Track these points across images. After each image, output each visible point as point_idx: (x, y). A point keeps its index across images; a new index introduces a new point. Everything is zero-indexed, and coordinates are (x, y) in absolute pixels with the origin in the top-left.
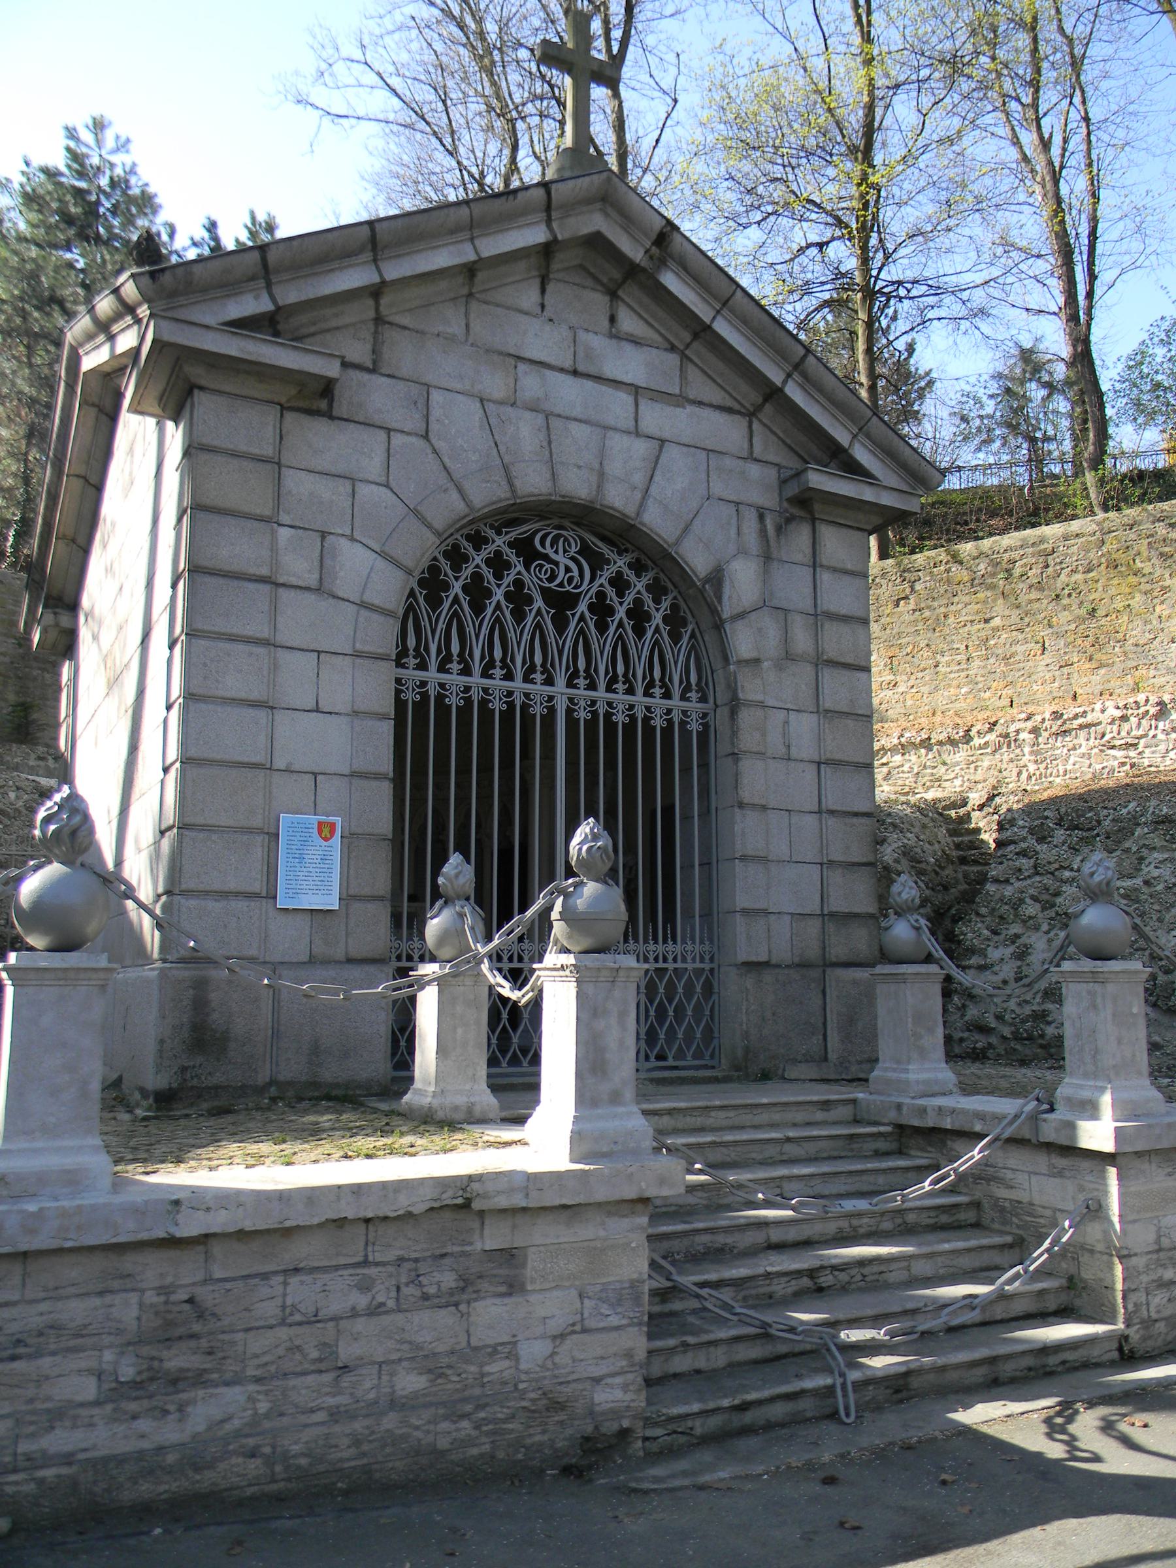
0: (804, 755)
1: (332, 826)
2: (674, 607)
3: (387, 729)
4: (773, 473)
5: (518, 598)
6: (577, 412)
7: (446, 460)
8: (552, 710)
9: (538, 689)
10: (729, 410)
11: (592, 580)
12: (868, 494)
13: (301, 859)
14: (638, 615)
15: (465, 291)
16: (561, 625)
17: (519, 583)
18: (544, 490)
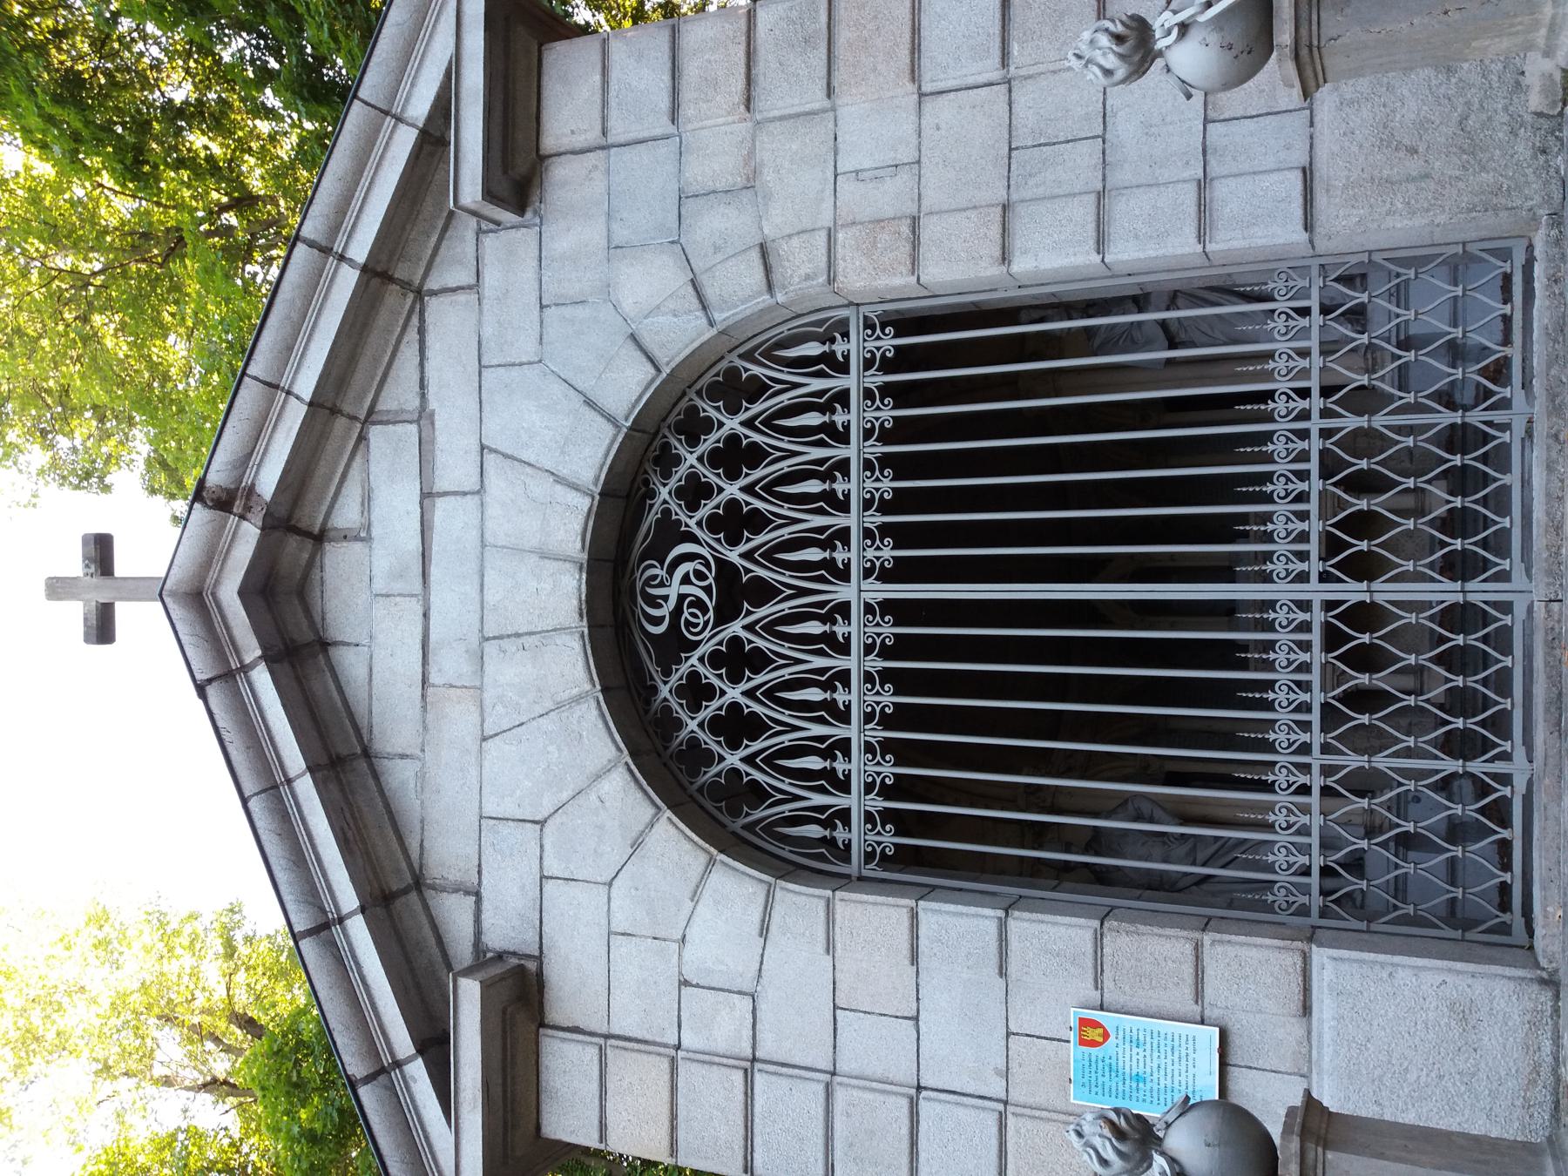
0: (909, 128)
1: (1085, 1023)
2: (713, 392)
4: (489, 241)
5: (736, 660)
6: (472, 590)
7: (565, 796)
8: (888, 607)
9: (854, 629)
10: (422, 331)
11: (693, 539)
13: (1138, 1078)
14: (734, 457)
15: (362, 765)
16: (763, 592)
17: (715, 660)
18: (577, 645)
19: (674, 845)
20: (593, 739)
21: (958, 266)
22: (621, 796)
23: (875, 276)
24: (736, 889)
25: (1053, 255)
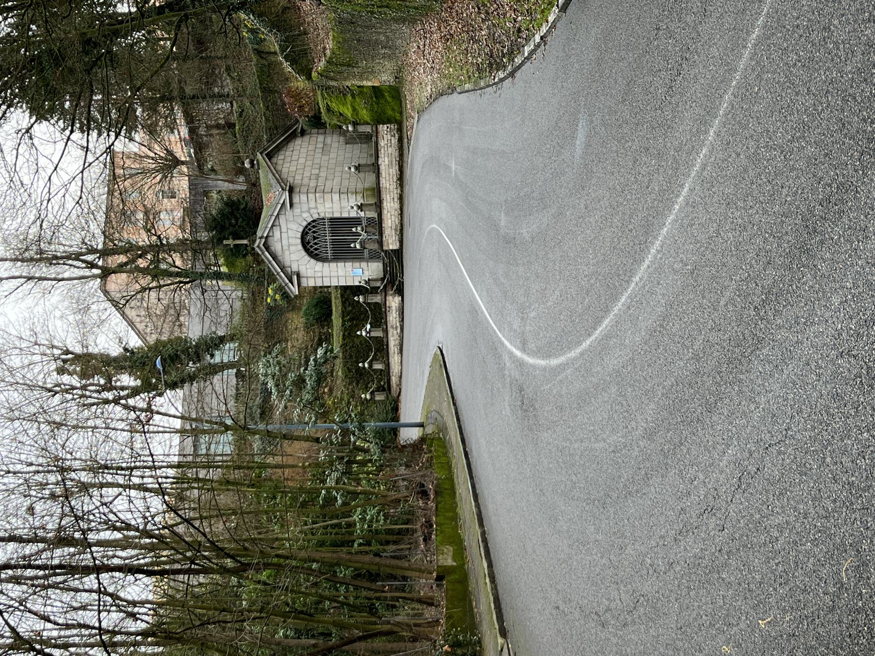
5: (316, 244)
14: (314, 227)
19: (313, 261)
20: (303, 253)
21: (337, 215)
22: (307, 258)
23: (329, 216)
24: (320, 264)
25: (345, 215)
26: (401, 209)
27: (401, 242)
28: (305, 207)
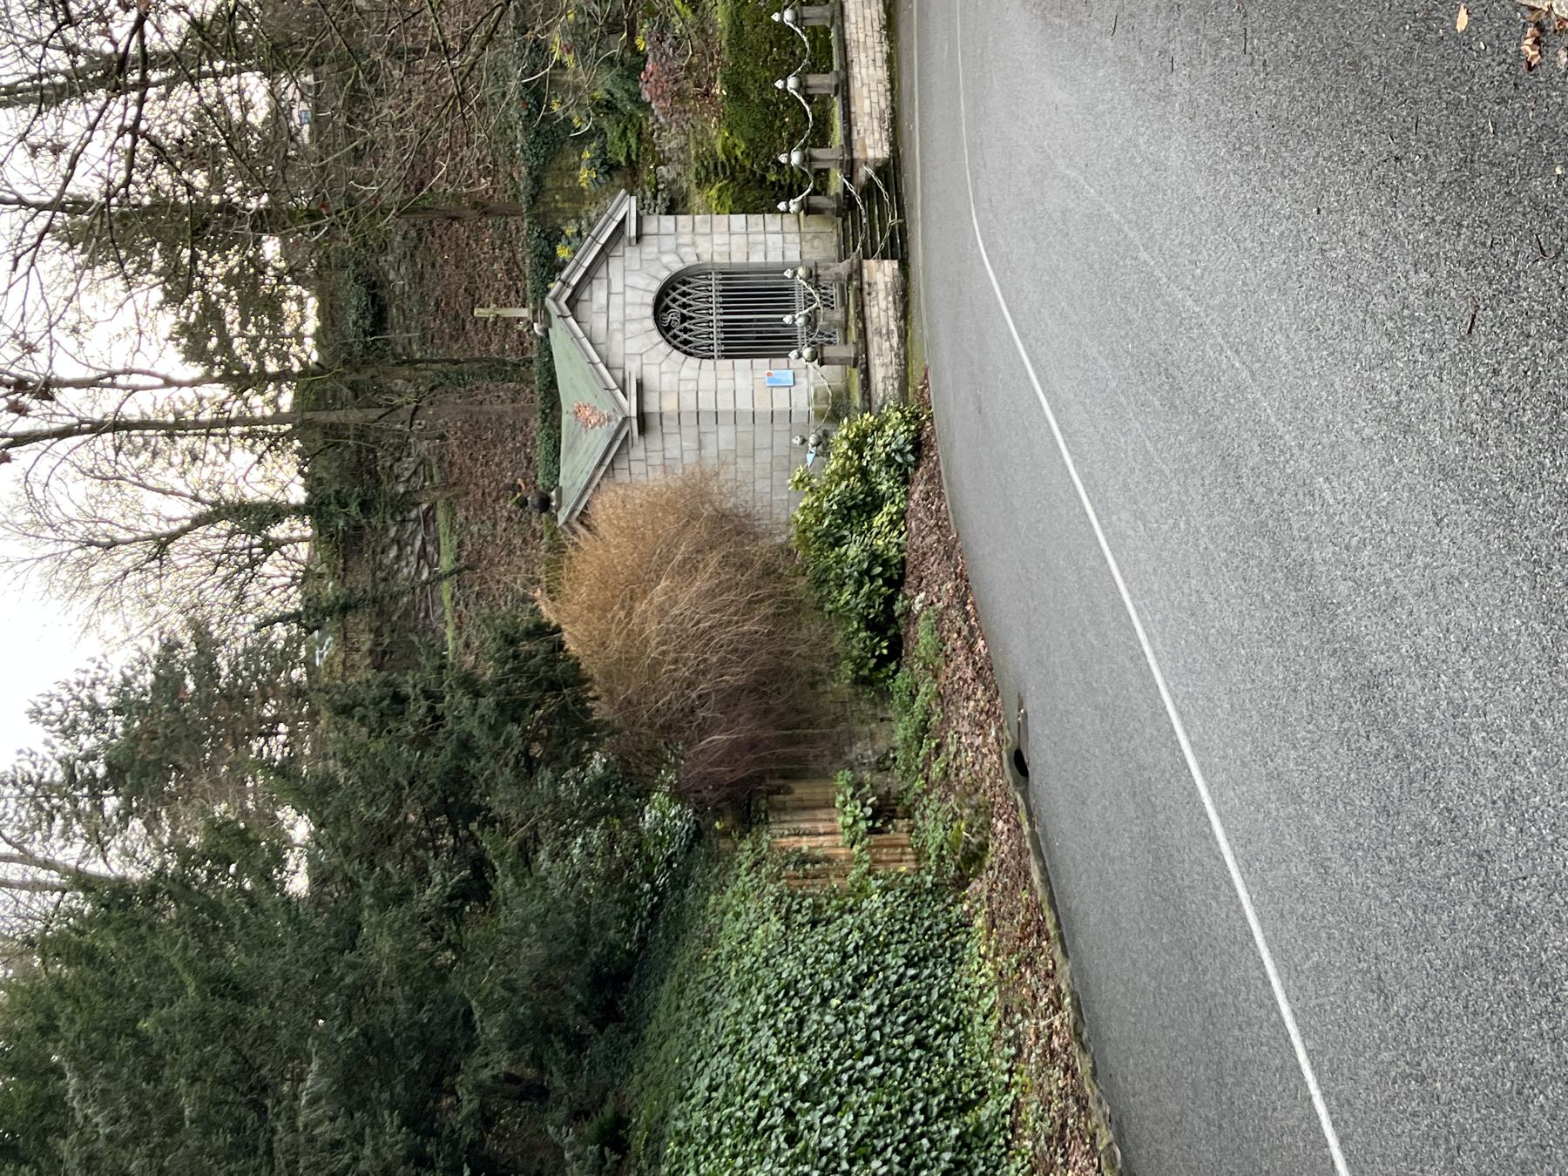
3: (737, 361)
5: (685, 330)
12: (634, 215)
14: (684, 294)
25: (757, 258)
26: (893, 80)
27: (895, 144)
28: (668, 243)
